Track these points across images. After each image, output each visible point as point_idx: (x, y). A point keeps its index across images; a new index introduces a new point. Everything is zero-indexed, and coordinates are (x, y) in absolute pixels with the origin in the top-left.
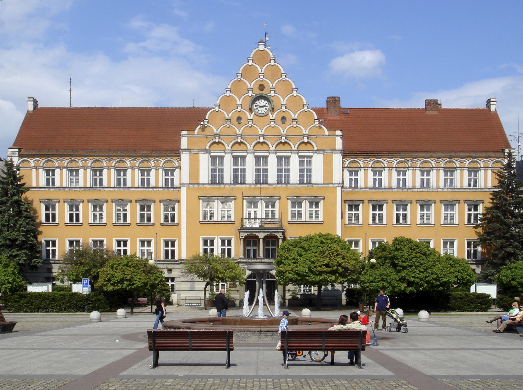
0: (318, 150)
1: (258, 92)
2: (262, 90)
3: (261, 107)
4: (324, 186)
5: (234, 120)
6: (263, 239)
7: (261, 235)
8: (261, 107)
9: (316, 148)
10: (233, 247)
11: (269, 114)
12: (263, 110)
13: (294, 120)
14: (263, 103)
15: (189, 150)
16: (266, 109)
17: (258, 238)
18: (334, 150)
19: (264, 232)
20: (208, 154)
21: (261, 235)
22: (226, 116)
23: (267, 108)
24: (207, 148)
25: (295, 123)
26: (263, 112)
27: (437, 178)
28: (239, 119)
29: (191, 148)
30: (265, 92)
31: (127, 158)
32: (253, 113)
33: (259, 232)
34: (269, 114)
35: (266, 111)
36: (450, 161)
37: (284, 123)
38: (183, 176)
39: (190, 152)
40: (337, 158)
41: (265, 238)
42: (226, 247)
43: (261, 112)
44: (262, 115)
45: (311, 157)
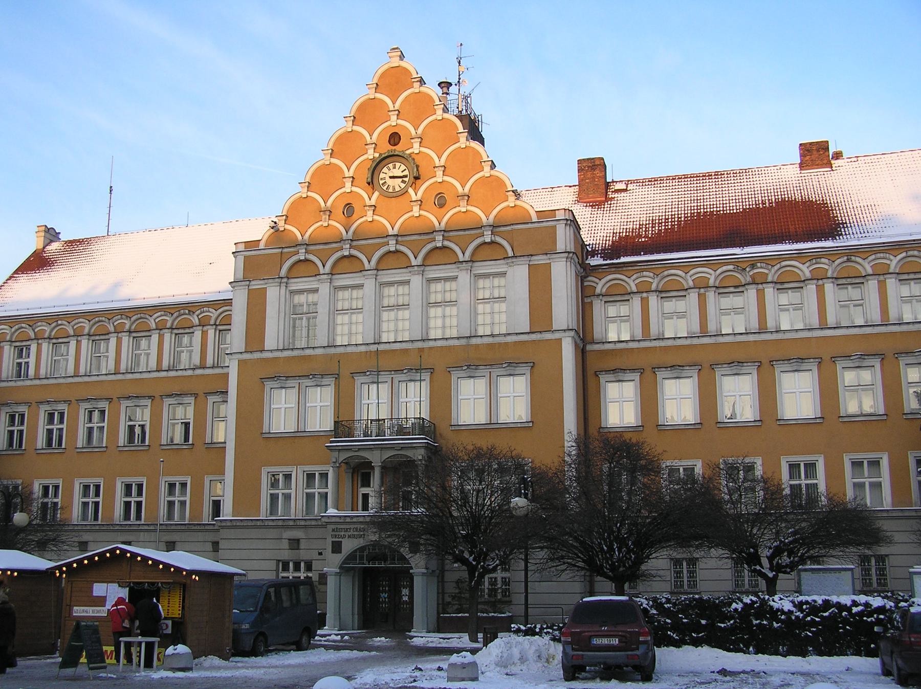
1: (386, 148)
2: (395, 145)
4: (534, 337)
6: (384, 468)
7: (376, 459)
11: (411, 191)
12: (397, 184)
14: (399, 169)
16: (403, 182)
17: (368, 465)
23: (406, 179)
25: (463, 203)
26: (397, 189)
32: (376, 194)
34: (411, 191)
35: (403, 185)
36: (849, 260)
43: (394, 188)
44: (395, 195)
45: (503, 274)
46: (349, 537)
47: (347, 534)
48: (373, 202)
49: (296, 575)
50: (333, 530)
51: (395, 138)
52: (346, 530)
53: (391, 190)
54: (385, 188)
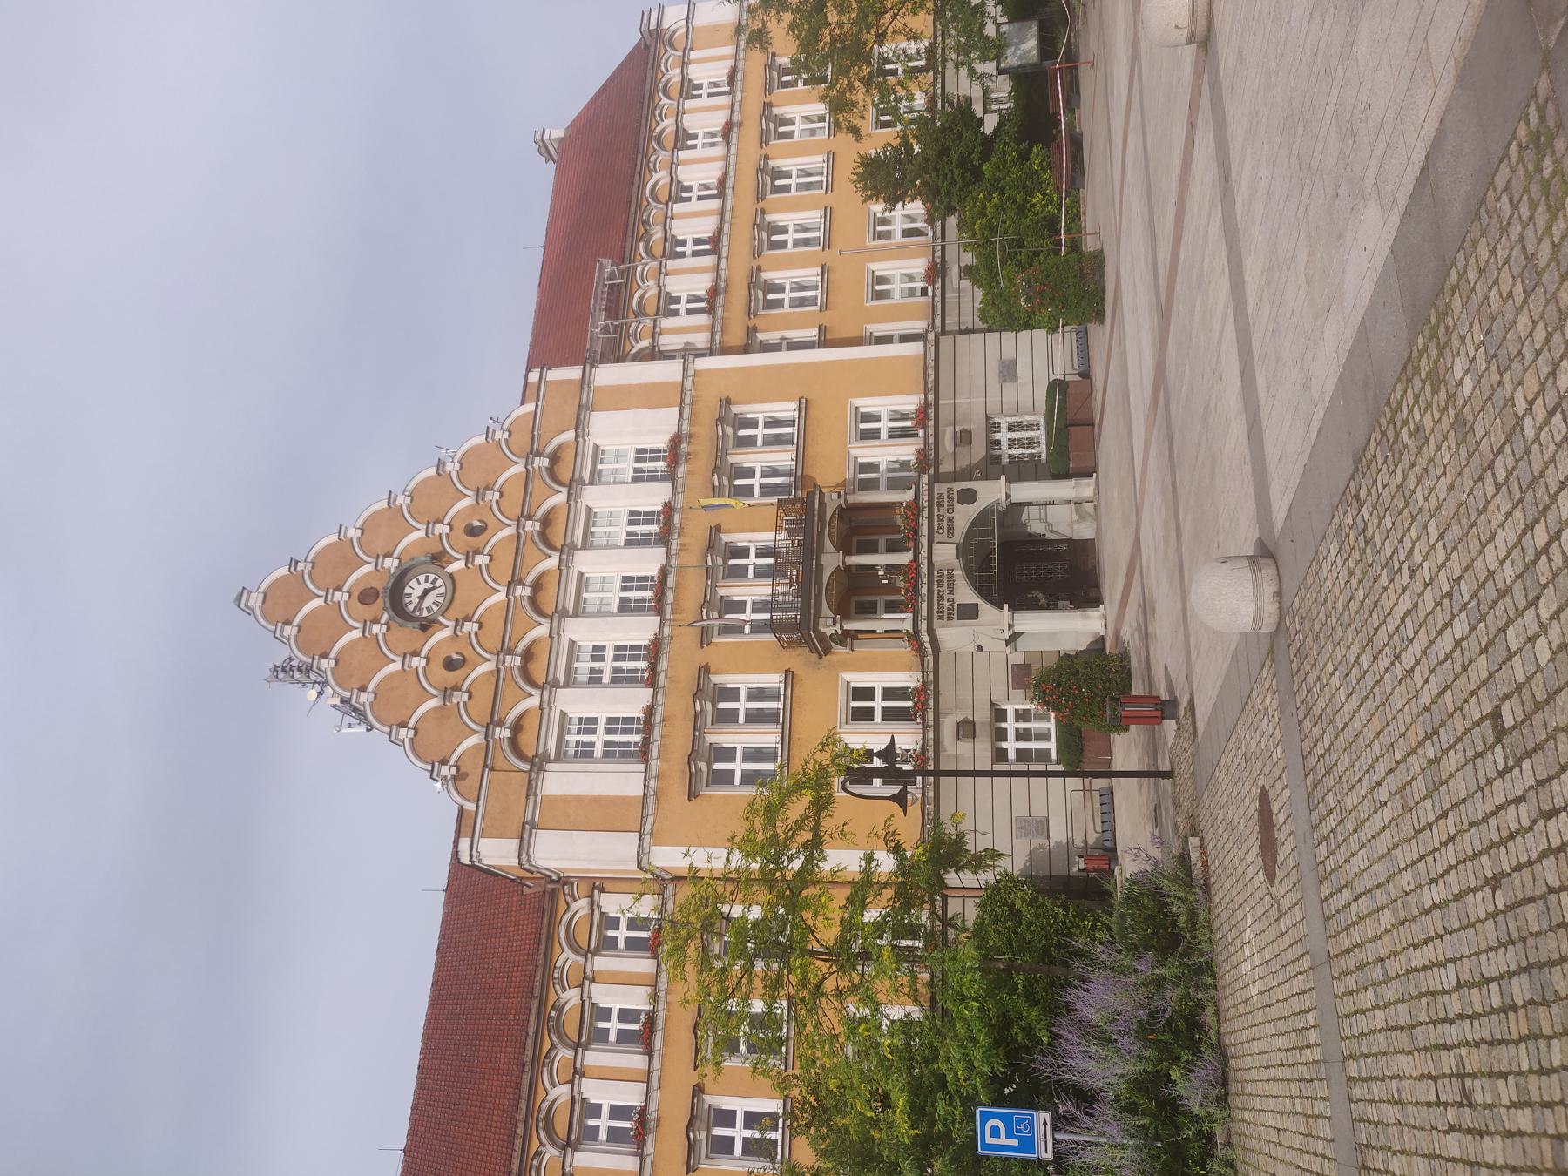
0: (579, 426)
3: (426, 592)
5: (452, 677)
7: (832, 560)
8: (426, 592)
9: (571, 435)
10: (878, 681)
11: (451, 568)
13: (479, 495)
14: (414, 589)
15: (525, 833)
18: (584, 382)
19: (821, 550)
20: (549, 766)
21: (832, 560)
22: (433, 703)
24: (526, 767)
27: (699, 169)
28: (450, 665)
29: (517, 826)
30: (382, 584)
31: (541, 1093)
32: (441, 619)
33: (820, 567)
34: (451, 568)
37: (483, 529)
38: (609, 853)
39: (533, 827)
40: (607, 375)
41: (845, 547)
42: (878, 704)
46: (951, 592)
47: (946, 596)
48: (451, 624)
49: (1011, 735)
50: (941, 618)
51: (367, 596)
52: (941, 597)
53: (441, 600)
54: (435, 608)
